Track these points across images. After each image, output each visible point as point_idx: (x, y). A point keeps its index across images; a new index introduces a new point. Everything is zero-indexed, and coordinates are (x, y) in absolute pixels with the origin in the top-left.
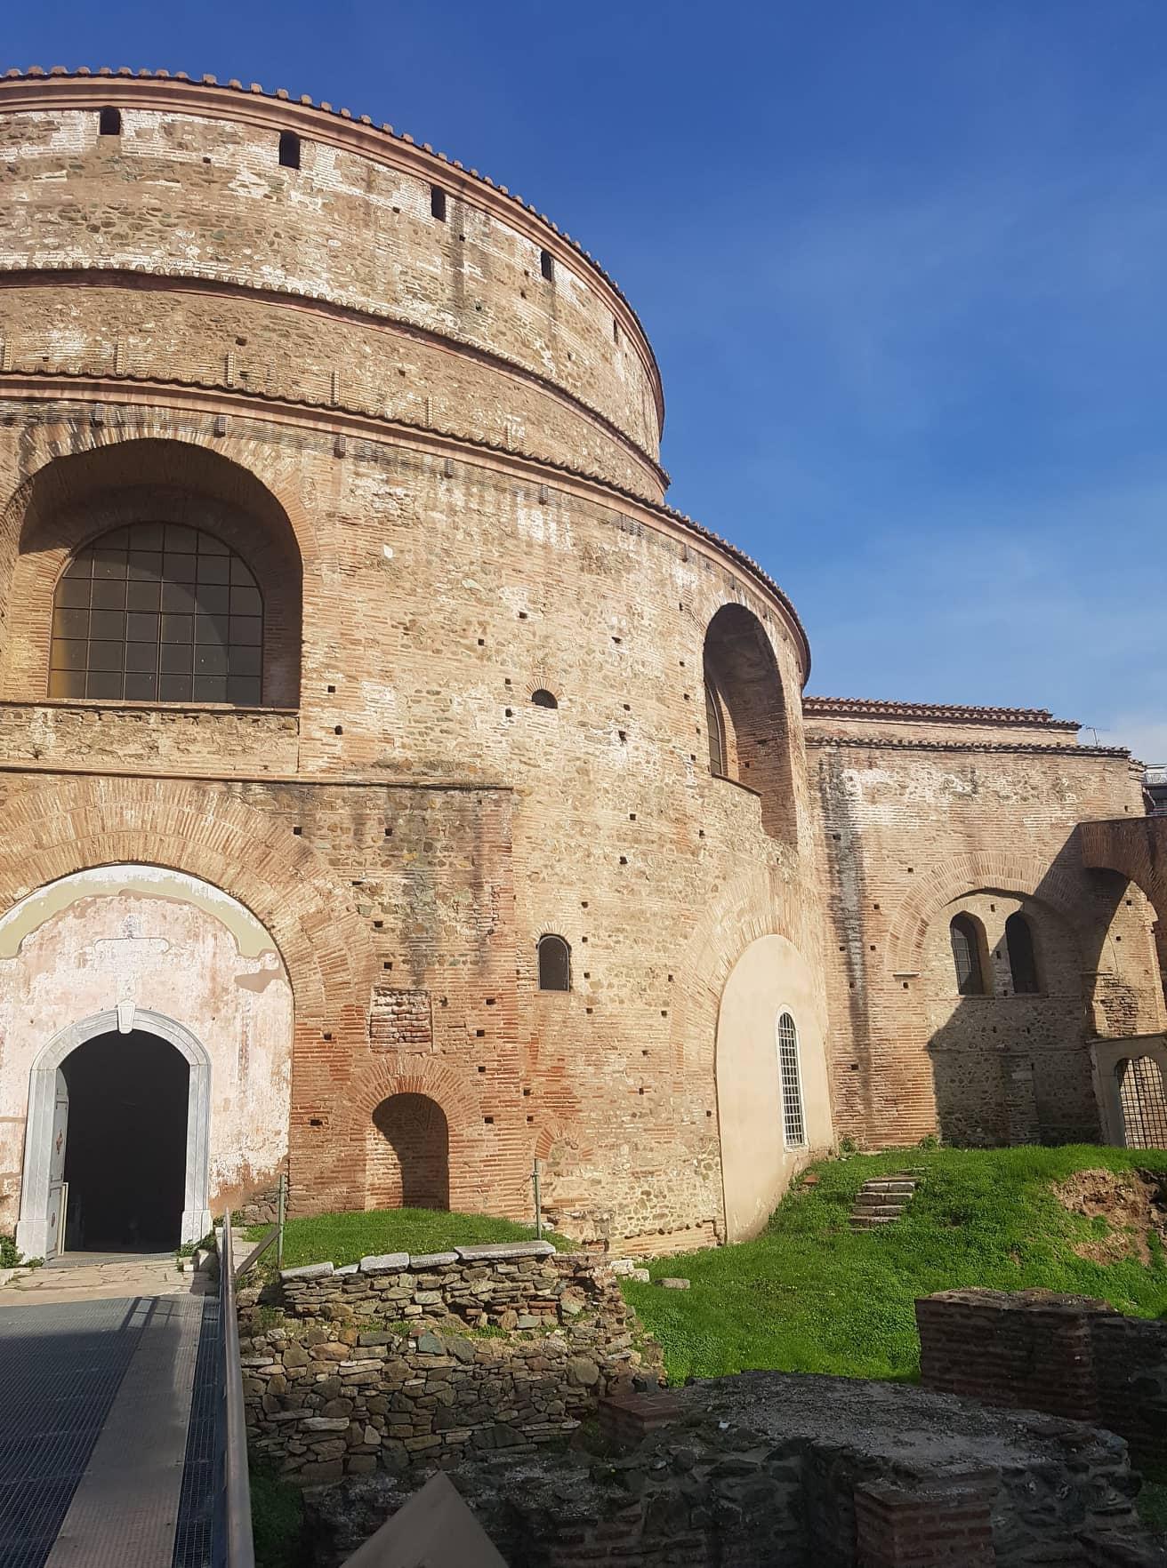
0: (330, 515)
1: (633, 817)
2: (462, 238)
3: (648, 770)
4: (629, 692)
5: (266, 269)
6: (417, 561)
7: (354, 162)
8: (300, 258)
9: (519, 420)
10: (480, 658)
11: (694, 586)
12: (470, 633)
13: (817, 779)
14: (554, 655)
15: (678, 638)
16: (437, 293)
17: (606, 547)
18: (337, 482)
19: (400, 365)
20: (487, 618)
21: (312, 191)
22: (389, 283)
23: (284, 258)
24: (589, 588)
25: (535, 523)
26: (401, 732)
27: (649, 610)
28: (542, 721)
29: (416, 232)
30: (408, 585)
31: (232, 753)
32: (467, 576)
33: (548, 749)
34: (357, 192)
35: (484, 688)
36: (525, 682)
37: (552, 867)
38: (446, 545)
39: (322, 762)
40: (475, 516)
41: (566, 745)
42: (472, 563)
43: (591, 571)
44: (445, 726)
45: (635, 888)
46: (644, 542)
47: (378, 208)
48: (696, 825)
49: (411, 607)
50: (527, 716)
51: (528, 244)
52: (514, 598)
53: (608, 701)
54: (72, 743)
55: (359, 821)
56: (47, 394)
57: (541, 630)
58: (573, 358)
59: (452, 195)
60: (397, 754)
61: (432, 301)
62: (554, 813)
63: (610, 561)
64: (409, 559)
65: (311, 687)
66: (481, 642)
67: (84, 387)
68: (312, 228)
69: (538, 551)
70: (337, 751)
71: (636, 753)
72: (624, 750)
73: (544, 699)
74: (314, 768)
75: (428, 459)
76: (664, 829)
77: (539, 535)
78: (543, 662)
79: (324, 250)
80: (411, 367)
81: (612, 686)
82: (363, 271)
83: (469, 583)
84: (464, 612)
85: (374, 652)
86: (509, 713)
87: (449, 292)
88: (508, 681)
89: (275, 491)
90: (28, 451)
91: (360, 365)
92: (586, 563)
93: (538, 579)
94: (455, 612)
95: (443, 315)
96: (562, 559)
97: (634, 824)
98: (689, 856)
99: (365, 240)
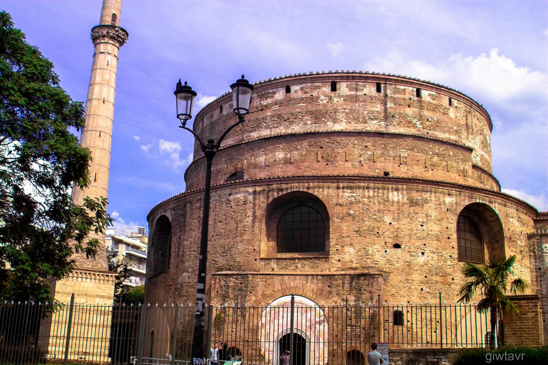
0: (336, 204)
1: (426, 277)
2: (387, 96)
3: (431, 262)
4: (426, 240)
5: (328, 123)
6: (359, 213)
7: (352, 84)
8: (338, 117)
9: (405, 151)
10: (377, 237)
11: (453, 202)
12: (375, 231)
13: (532, 248)
14: (400, 233)
15: (446, 220)
16: (378, 117)
17: (418, 198)
18: (338, 195)
19: (365, 144)
20: (379, 225)
21: (339, 96)
22: (363, 118)
23: (333, 119)
24: (412, 212)
25: (394, 196)
26: (355, 259)
27: (434, 214)
28: (396, 252)
29: (371, 99)
30: (357, 220)
31: (314, 268)
32: (374, 215)
33: (398, 260)
34: (353, 93)
35: (379, 245)
36: (391, 241)
37: (398, 292)
38: (367, 207)
39: (335, 269)
40: (376, 197)
41: (403, 258)
42: (375, 211)
43: (413, 206)
44: (367, 257)
45: (426, 297)
46: (433, 194)
47: (360, 96)
48: (450, 276)
49: (358, 226)
50: (391, 251)
51: (411, 89)
52: (388, 219)
53: (418, 244)
54: (280, 267)
55: (343, 284)
56: (271, 183)
57: (396, 227)
58: (429, 120)
59: (383, 83)
60: (354, 265)
61: (376, 119)
62: (399, 278)
63: (420, 202)
64: (357, 213)
65: (332, 250)
66: (378, 233)
67: (279, 181)
68: (341, 108)
69: (396, 204)
70: (339, 266)
71: (427, 258)
72: (423, 258)
73: (397, 246)
74: (333, 271)
75: (362, 184)
76: (438, 279)
77: (396, 199)
78: (397, 236)
79: (344, 114)
80: (369, 144)
81: (419, 239)
82: (356, 116)
83: (375, 217)
84: (373, 225)
85: (348, 239)
86: (386, 251)
87: (383, 115)
88: (386, 243)
89: (323, 200)
90: (268, 197)
91: (354, 147)
92: (412, 204)
93: (395, 212)
94: (370, 226)
95: (381, 123)
96: (403, 204)
97: (426, 279)
98: (447, 286)
99: (356, 107)
